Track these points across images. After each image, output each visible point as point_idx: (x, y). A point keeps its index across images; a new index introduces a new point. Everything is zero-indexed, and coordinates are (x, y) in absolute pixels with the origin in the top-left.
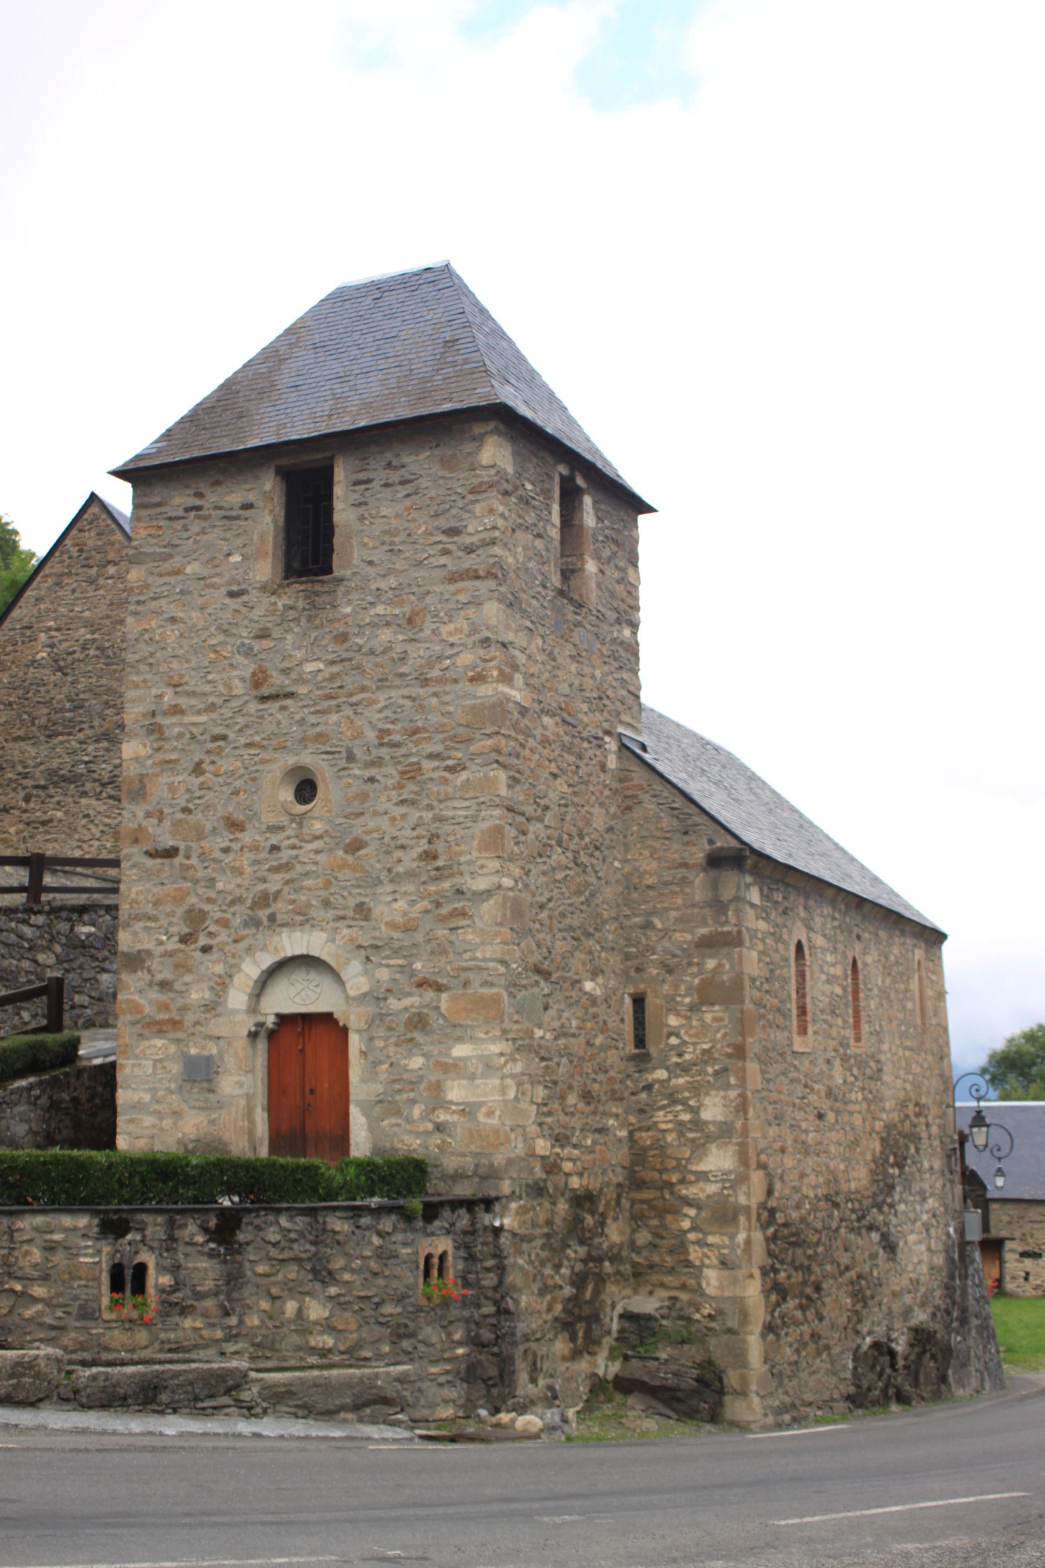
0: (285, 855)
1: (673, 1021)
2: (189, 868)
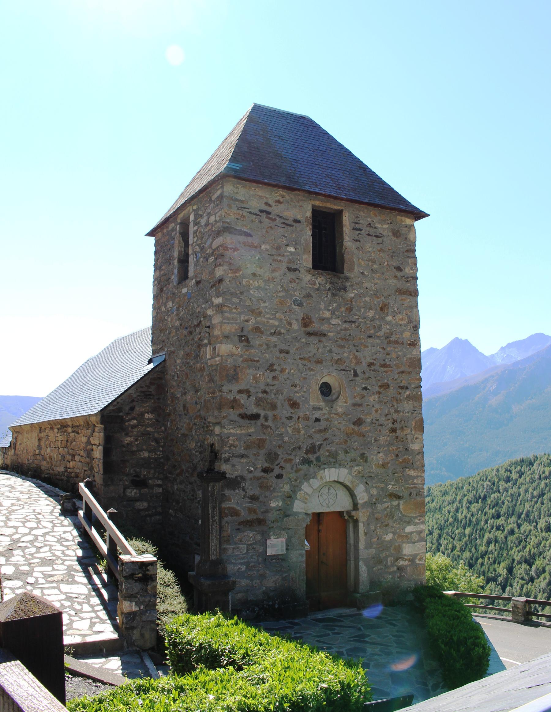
2: (267, 427)
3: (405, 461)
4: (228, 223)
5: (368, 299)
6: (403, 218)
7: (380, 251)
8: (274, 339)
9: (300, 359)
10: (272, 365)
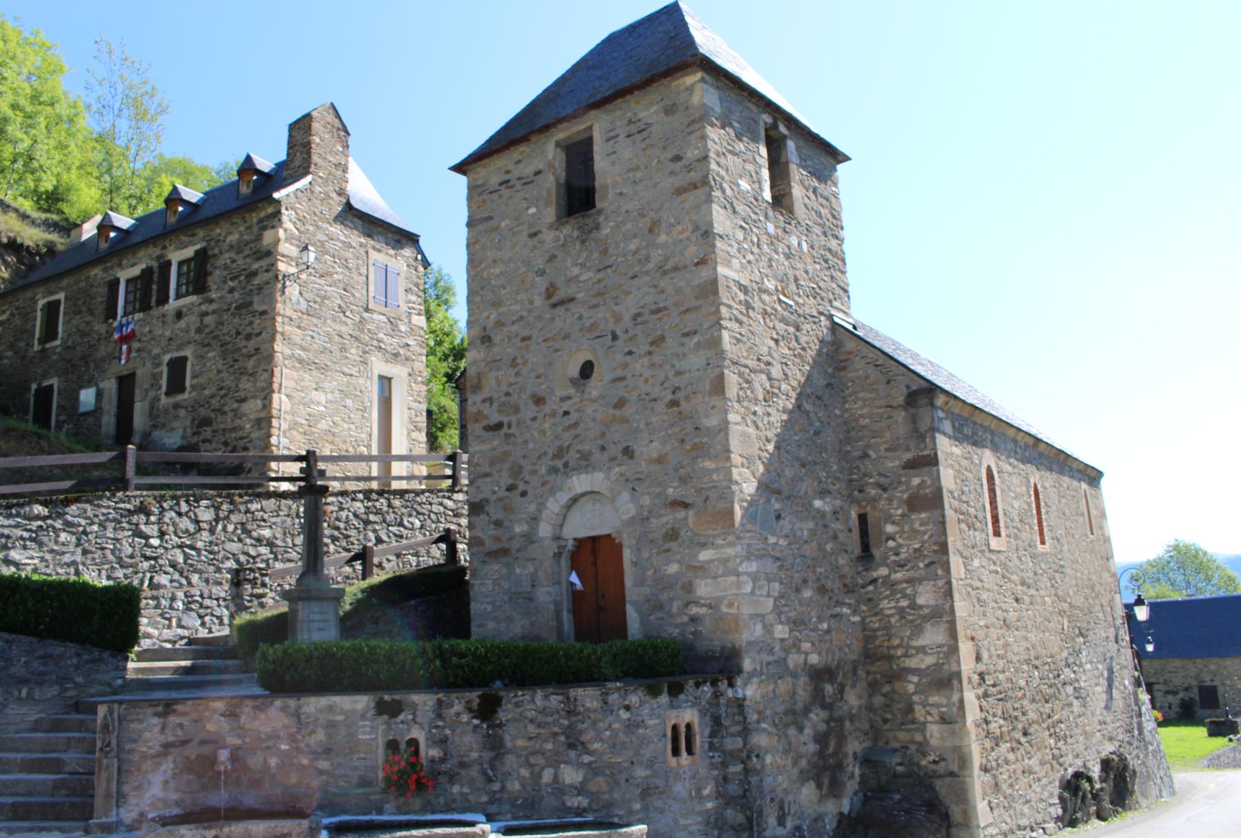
0: (574, 417)
1: (890, 529)
3: (695, 447)
6: (681, 81)
9: (545, 341)
10: (514, 359)
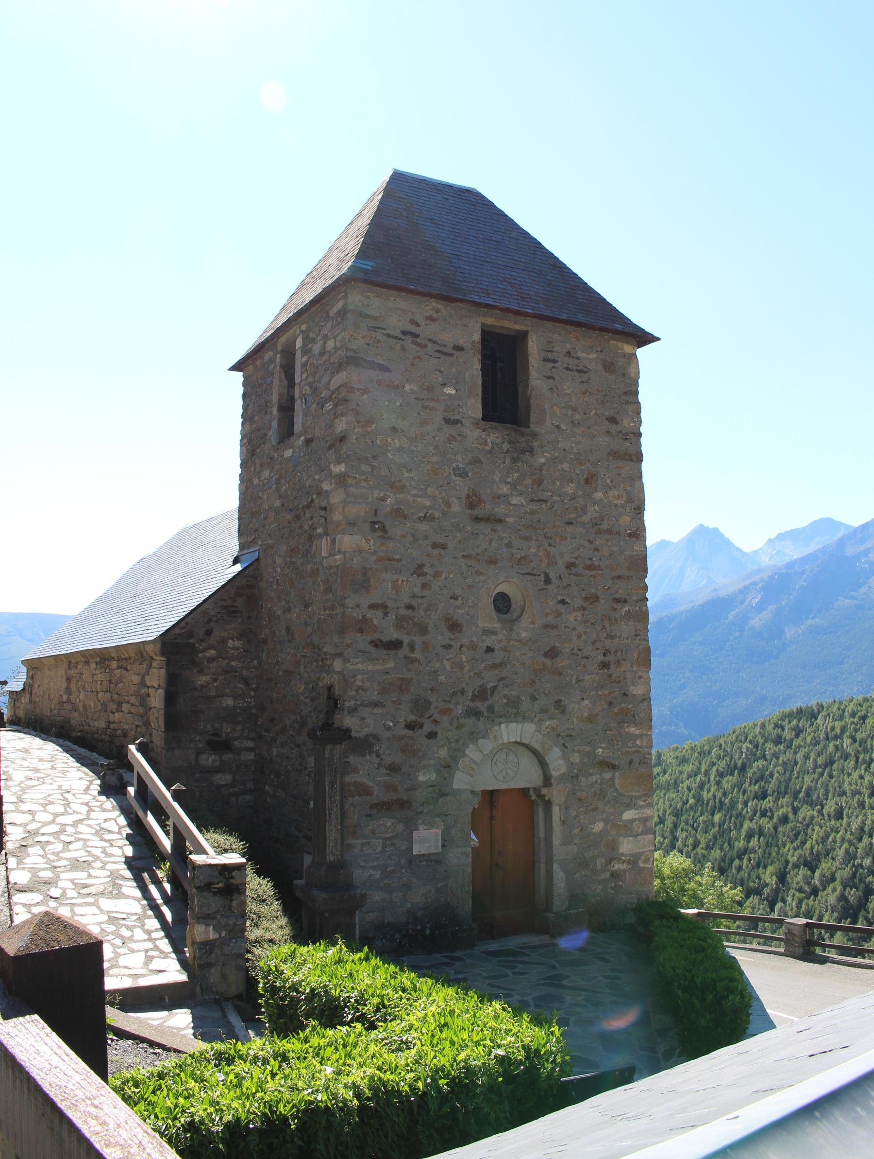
4: (355, 351)
5: (566, 466)
6: (620, 344)
7: (584, 393)
8: (424, 527)
9: (464, 557)
10: (421, 566)
